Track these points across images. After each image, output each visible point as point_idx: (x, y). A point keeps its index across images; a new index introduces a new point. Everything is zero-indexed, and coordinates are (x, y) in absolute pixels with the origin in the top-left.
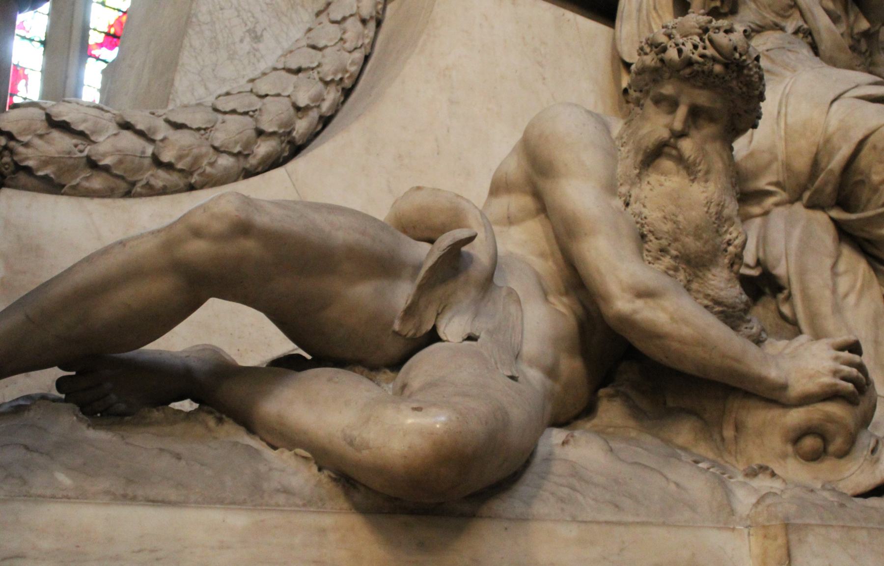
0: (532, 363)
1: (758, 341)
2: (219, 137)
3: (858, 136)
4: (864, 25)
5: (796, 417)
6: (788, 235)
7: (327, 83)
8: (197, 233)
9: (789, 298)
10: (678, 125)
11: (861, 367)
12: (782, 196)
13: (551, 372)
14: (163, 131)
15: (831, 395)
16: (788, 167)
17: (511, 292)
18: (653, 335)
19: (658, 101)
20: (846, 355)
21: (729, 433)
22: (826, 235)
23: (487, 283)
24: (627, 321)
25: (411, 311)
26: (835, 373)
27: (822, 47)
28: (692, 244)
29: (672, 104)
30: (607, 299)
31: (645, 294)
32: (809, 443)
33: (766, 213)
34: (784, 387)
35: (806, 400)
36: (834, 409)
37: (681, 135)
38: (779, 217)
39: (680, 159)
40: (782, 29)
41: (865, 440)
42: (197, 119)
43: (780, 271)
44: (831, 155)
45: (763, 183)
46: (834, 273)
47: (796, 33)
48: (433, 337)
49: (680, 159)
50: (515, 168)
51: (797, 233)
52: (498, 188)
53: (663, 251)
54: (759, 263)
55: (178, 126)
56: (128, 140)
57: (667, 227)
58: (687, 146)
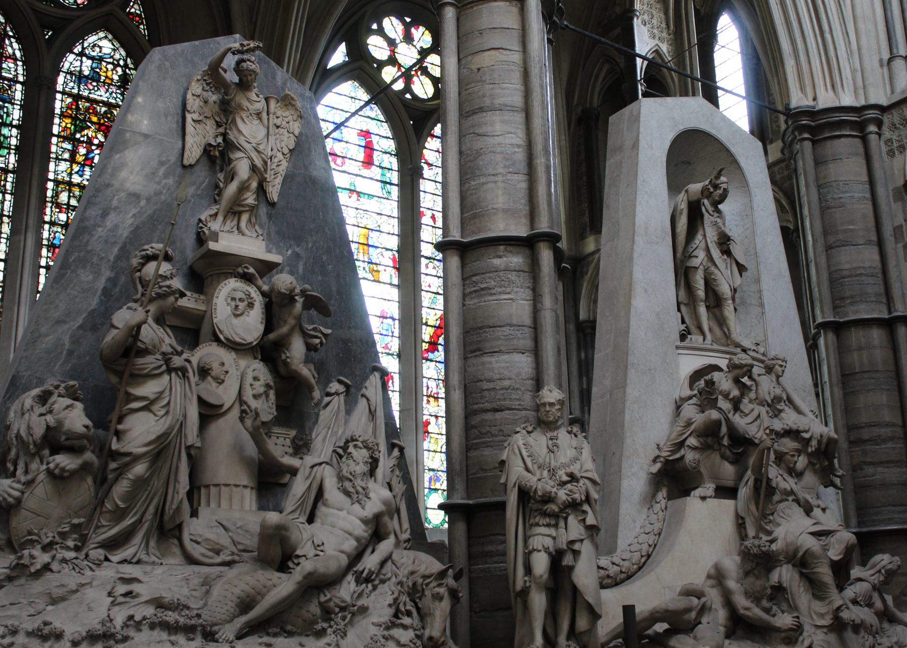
0: (721, 625)
1: (774, 616)
2: (634, 561)
3: (804, 549)
4: (826, 463)
5: (783, 635)
6: (787, 575)
7: (655, 535)
8: (658, 612)
9: (787, 593)
10: (754, 567)
11: (799, 622)
12: (786, 561)
13: (725, 627)
14: (622, 563)
15: (791, 629)
16: (787, 553)
17: (716, 609)
18: (748, 617)
19: (749, 559)
20: (795, 619)
21: (768, 638)
22: (797, 576)
23: (710, 609)
24: (743, 615)
25: (695, 619)
26: (792, 624)
27: (801, 504)
28: (758, 595)
29: (753, 561)
30: (738, 610)
31: (747, 609)
32: (787, 640)
33: (781, 566)
34: (780, 628)
35: (785, 631)
36: (791, 633)
37: (755, 569)
38: (785, 566)
39: (754, 574)
40: (788, 500)
41: (801, 638)
42: (627, 556)
43: (785, 585)
44: (799, 552)
45: (781, 558)
46: (799, 586)
47: (793, 500)
48: (700, 623)
49: (754, 574)
50: (713, 572)
51: (789, 574)
52: (709, 577)
53: (751, 596)
54: (779, 582)
55: (624, 560)
56: (616, 568)
57: (751, 591)
58: (756, 572)
